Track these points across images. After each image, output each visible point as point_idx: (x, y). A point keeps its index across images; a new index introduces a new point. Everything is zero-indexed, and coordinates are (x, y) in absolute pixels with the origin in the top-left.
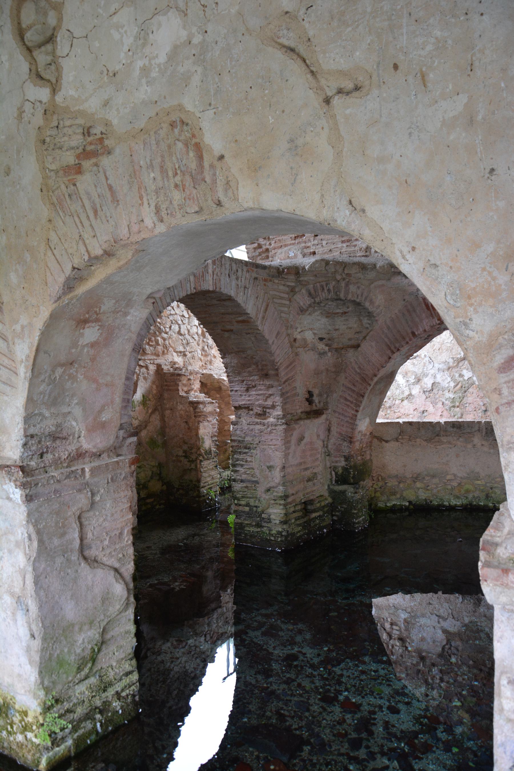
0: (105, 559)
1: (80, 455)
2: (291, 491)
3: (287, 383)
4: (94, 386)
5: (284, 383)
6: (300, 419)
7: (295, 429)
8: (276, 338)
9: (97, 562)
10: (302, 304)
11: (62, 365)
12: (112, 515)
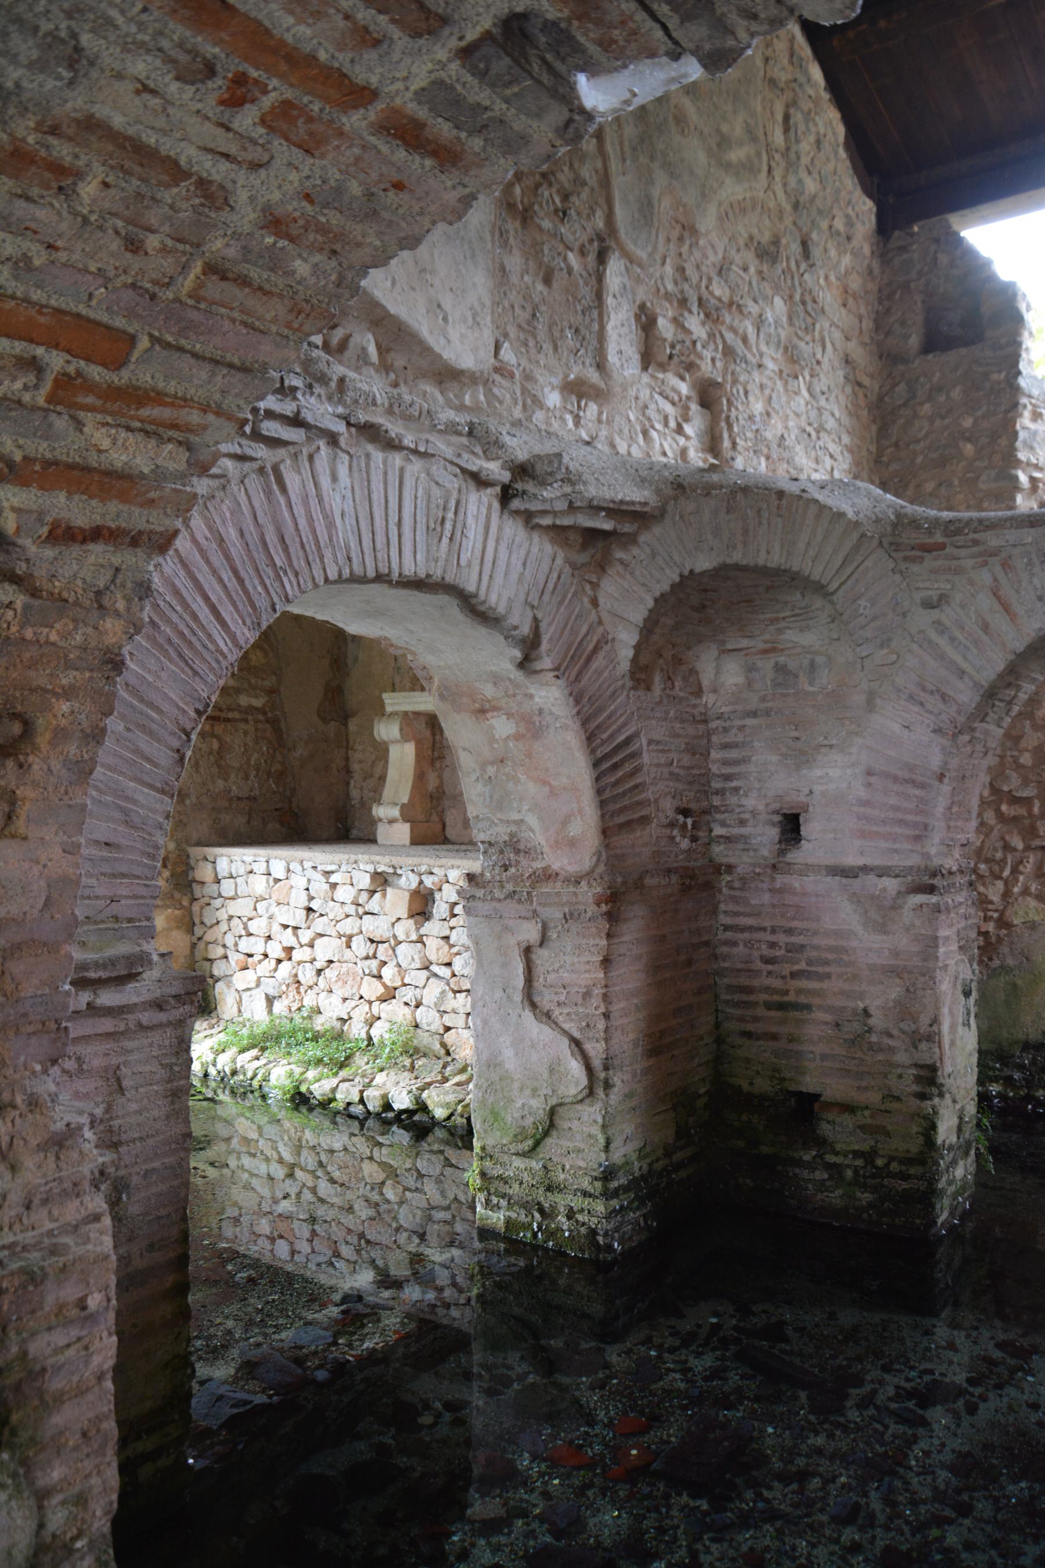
0: (561, 1018)
1: (548, 876)
4: (546, 789)
9: (550, 1018)
11: (492, 763)
12: (573, 964)
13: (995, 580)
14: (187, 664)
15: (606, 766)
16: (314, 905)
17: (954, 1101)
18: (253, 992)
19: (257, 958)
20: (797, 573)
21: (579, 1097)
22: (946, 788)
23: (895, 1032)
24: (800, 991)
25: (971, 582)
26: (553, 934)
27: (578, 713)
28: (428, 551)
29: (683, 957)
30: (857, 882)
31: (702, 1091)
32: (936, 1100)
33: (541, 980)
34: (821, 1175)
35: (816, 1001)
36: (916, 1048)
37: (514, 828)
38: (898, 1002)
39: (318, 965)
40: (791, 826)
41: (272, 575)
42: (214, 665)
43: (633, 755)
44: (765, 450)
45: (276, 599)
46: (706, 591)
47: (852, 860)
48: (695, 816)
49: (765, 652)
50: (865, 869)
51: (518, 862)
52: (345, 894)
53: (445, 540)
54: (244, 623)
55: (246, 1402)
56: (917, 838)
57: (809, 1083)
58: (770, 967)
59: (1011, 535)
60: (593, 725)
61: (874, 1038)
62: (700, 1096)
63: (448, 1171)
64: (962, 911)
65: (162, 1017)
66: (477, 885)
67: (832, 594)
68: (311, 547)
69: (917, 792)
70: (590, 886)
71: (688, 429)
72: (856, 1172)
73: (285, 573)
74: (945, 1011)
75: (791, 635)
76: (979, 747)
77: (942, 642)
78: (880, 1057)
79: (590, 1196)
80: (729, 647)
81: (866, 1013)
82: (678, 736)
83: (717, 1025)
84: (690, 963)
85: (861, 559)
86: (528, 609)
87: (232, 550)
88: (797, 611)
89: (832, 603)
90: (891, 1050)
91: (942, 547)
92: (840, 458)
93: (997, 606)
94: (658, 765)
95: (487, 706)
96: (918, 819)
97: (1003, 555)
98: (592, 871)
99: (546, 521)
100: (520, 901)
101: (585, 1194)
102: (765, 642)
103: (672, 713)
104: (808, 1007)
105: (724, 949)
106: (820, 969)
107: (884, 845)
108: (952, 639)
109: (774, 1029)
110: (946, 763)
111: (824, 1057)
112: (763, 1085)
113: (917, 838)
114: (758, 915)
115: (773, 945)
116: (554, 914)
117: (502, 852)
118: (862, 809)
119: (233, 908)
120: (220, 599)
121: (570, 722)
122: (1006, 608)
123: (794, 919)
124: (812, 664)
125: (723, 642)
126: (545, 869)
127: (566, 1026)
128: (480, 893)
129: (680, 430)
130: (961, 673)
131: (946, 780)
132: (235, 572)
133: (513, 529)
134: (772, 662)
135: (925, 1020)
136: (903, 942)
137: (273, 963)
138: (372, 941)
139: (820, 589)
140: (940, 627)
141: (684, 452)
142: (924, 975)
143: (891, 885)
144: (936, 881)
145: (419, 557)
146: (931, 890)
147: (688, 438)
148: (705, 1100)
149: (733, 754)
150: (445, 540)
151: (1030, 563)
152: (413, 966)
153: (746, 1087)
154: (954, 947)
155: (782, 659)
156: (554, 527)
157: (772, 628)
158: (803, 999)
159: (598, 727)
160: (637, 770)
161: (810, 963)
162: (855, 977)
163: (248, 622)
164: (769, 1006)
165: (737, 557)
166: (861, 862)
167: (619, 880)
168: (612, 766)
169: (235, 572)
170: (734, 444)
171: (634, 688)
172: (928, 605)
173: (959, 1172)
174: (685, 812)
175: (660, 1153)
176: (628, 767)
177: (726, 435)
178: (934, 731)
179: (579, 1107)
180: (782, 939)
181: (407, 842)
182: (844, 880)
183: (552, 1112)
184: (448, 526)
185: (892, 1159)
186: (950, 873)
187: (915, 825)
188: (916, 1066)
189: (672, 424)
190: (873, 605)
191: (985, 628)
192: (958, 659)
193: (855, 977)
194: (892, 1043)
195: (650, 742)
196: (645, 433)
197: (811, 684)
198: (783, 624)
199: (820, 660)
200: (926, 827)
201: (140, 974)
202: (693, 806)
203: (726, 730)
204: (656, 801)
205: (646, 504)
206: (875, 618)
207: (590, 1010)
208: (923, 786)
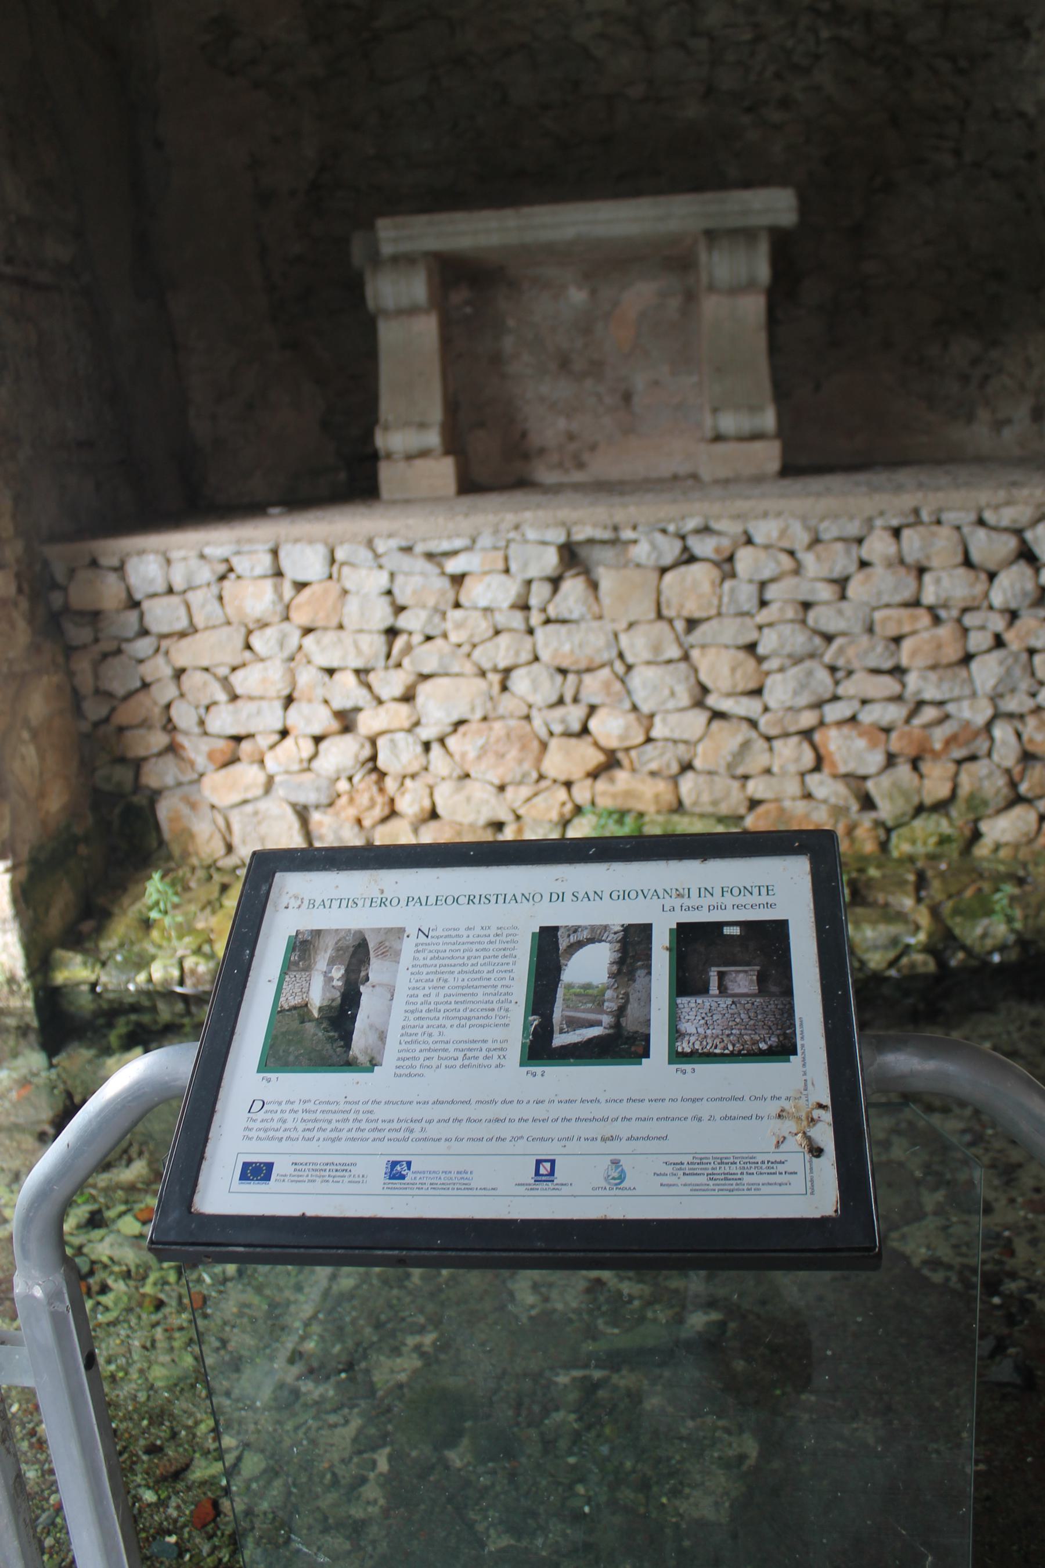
16: (403, 622)
18: (263, 805)
19: (263, 742)
39: (426, 733)
52: (492, 591)
119: (212, 648)
137: (307, 748)
138: (563, 672)
152: (671, 704)
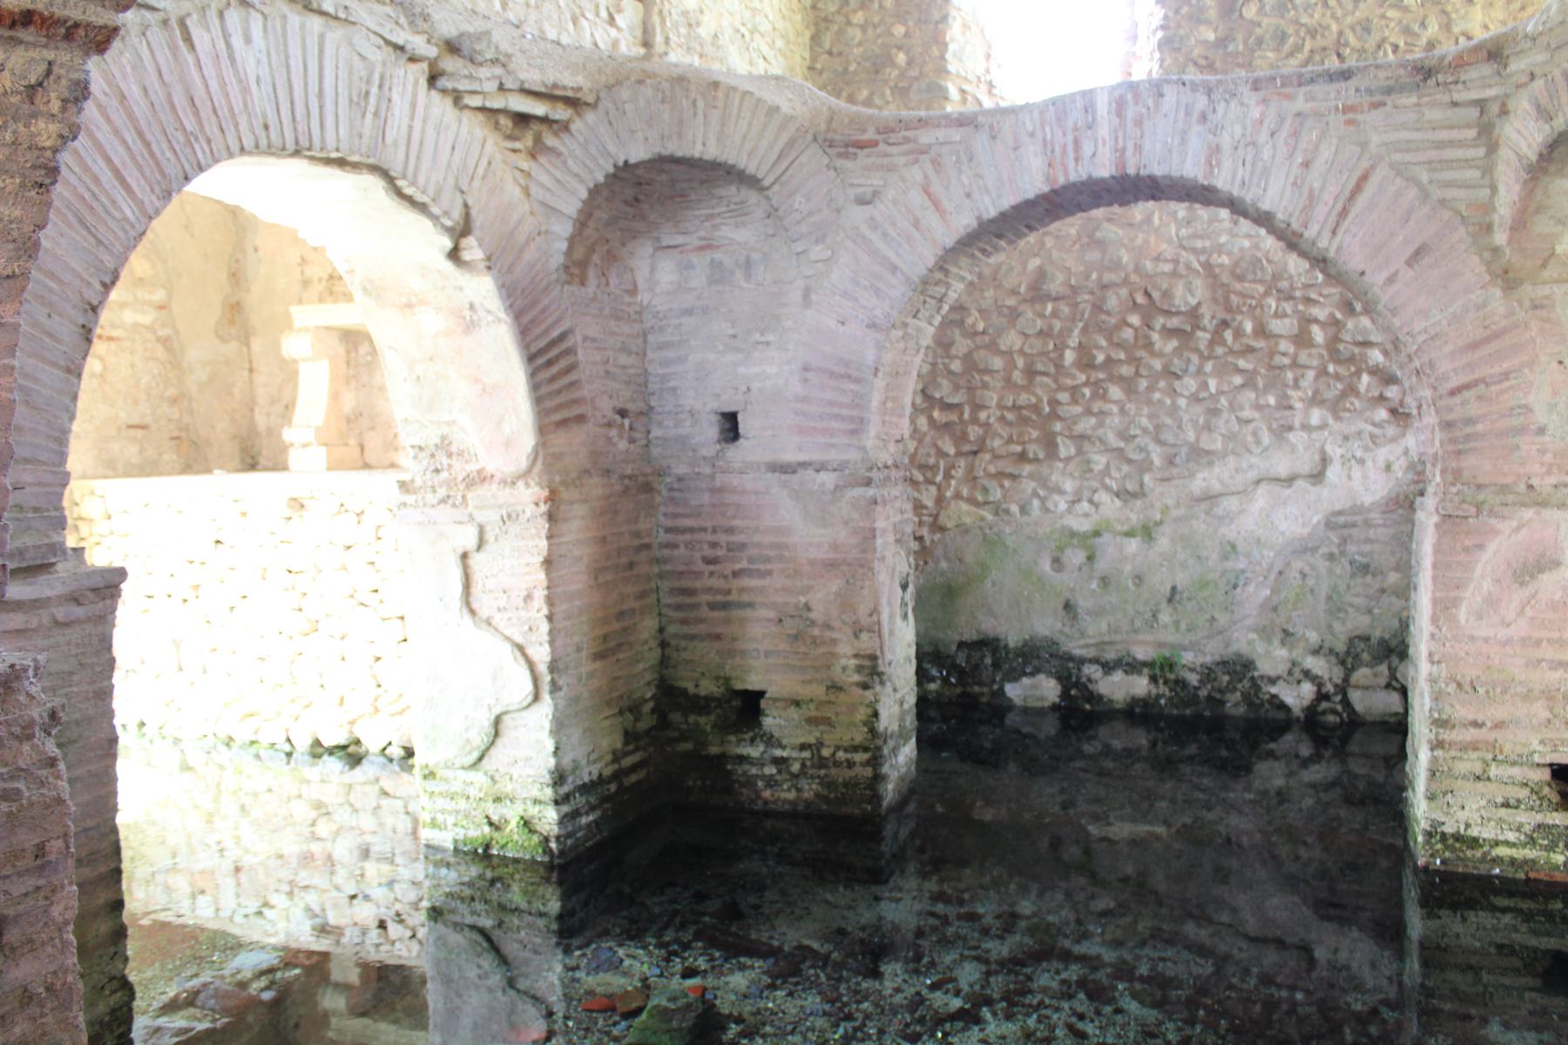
1: (482, 478)
2: (1462, 712)
3: (1467, 394)
5: (1452, 393)
6: (1544, 504)
7: (1495, 532)
8: (1410, 263)
10: (1525, 149)
13: (926, 177)
14: (90, 232)
15: (541, 361)
17: (895, 690)
20: (733, 166)
21: (525, 703)
22: (880, 382)
23: (836, 624)
24: (742, 590)
25: (903, 180)
26: (490, 536)
27: (511, 306)
28: (351, 127)
29: (624, 560)
30: (795, 479)
31: (649, 695)
32: (878, 688)
33: (480, 586)
34: (770, 770)
35: (759, 599)
36: (856, 636)
37: (445, 430)
38: (838, 594)
40: (730, 426)
41: (182, 139)
42: (121, 234)
43: (569, 352)
44: (698, 48)
45: (187, 167)
46: (640, 184)
47: (790, 456)
48: (634, 416)
49: (701, 248)
50: (804, 465)
51: (450, 466)
53: (369, 116)
54: (152, 190)
55: (188, 1030)
56: (854, 432)
57: (753, 682)
58: (711, 568)
59: (941, 134)
60: (526, 319)
61: (816, 632)
62: (646, 701)
63: (385, 802)
64: (898, 504)
65: (79, 612)
66: (408, 491)
67: (768, 188)
68: (224, 112)
69: (852, 387)
70: (527, 485)
71: (620, 20)
72: (803, 765)
73: (196, 139)
74: (884, 601)
75: (727, 232)
76: (911, 344)
77: (875, 237)
78: (822, 650)
79: (540, 802)
80: (664, 243)
81: (808, 608)
82: (612, 334)
83: (661, 630)
84: (631, 565)
85: (795, 154)
86: (458, 195)
87: (135, 109)
88: (733, 207)
89: (767, 198)
90: (834, 642)
91: (875, 144)
92: (773, 62)
93: (928, 203)
94: (595, 363)
95: (414, 300)
96: (855, 413)
97: (933, 153)
98: (528, 471)
99: (475, 101)
100: (454, 505)
101: (536, 802)
102: (701, 239)
103: (607, 311)
104: (751, 605)
105: (666, 552)
106: (762, 567)
107: (821, 440)
108: (885, 235)
109: (718, 630)
110: (879, 357)
111: (767, 654)
112: (708, 688)
113: (854, 432)
114: (699, 515)
115: (714, 545)
116: (490, 517)
117: (433, 456)
118: (799, 406)
120: (124, 163)
121: (503, 315)
122: (937, 205)
123: (734, 517)
124: (748, 261)
125: (658, 239)
126: (479, 472)
127: (508, 632)
128: (410, 499)
129: (612, 21)
130: (894, 269)
131: (880, 374)
132: (140, 134)
133: (440, 106)
134: (708, 259)
135: (863, 609)
136: (842, 535)
139: (752, 182)
140: (874, 225)
141: (615, 44)
142: (862, 566)
143: (828, 479)
144: (874, 474)
145: (341, 131)
146: (868, 483)
147: (619, 29)
148: (651, 705)
149: (670, 354)
150: (369, 116)
151: (958, 161)
153: (691, 689)
154: (891, 538)
155: (718, 256)
156: (482, 109)
157: (707, 224)
158: (745, 598)
159: (532, 321)
160: (571, 368)
161: (750, 560)
162: (797, 573)
163: (157, 190)
164: (713, 606)
165: (675, 148)
166: (801, 457)
167: (557, 479)
168: (547, 359)
169: (140, 134)
170: (667, 39)
171: (568, 283)
172: (862, 201)
173: (901, 759)
174: (623, 413)
175: (609, 757)
176: (562, 364)
177: (658, 30)
178: (868, 326)
179: (524, 713)
180: (722, 538)
181: (324, 466)
182: (784, 477)
183: (497, 721)
184: (372, 100)
185: (838, 748)
186: (887, 467)
187: (851, 419)
188: (856, 656)
189: (604, 14)
190: (808, 200)
191: (916, 224)
192: (891, 254)
193: (797, 573)
194: (835, 635)
195: (585, 338)
196: (575, 21)
197: (747, 281)
198: (719, 220)
199: (756, 256)
200: (862, 420)
201: (52, 564)
202: (630, 406)
203: (662, 330)
204: (592, 400)
205: (580, 89)
206: (810, 214)
207: (533, 614)
208: (858, 381)
